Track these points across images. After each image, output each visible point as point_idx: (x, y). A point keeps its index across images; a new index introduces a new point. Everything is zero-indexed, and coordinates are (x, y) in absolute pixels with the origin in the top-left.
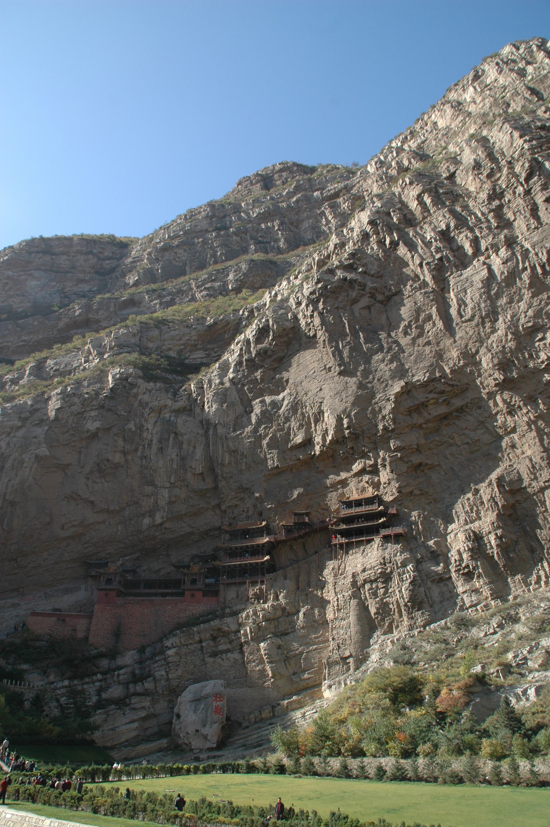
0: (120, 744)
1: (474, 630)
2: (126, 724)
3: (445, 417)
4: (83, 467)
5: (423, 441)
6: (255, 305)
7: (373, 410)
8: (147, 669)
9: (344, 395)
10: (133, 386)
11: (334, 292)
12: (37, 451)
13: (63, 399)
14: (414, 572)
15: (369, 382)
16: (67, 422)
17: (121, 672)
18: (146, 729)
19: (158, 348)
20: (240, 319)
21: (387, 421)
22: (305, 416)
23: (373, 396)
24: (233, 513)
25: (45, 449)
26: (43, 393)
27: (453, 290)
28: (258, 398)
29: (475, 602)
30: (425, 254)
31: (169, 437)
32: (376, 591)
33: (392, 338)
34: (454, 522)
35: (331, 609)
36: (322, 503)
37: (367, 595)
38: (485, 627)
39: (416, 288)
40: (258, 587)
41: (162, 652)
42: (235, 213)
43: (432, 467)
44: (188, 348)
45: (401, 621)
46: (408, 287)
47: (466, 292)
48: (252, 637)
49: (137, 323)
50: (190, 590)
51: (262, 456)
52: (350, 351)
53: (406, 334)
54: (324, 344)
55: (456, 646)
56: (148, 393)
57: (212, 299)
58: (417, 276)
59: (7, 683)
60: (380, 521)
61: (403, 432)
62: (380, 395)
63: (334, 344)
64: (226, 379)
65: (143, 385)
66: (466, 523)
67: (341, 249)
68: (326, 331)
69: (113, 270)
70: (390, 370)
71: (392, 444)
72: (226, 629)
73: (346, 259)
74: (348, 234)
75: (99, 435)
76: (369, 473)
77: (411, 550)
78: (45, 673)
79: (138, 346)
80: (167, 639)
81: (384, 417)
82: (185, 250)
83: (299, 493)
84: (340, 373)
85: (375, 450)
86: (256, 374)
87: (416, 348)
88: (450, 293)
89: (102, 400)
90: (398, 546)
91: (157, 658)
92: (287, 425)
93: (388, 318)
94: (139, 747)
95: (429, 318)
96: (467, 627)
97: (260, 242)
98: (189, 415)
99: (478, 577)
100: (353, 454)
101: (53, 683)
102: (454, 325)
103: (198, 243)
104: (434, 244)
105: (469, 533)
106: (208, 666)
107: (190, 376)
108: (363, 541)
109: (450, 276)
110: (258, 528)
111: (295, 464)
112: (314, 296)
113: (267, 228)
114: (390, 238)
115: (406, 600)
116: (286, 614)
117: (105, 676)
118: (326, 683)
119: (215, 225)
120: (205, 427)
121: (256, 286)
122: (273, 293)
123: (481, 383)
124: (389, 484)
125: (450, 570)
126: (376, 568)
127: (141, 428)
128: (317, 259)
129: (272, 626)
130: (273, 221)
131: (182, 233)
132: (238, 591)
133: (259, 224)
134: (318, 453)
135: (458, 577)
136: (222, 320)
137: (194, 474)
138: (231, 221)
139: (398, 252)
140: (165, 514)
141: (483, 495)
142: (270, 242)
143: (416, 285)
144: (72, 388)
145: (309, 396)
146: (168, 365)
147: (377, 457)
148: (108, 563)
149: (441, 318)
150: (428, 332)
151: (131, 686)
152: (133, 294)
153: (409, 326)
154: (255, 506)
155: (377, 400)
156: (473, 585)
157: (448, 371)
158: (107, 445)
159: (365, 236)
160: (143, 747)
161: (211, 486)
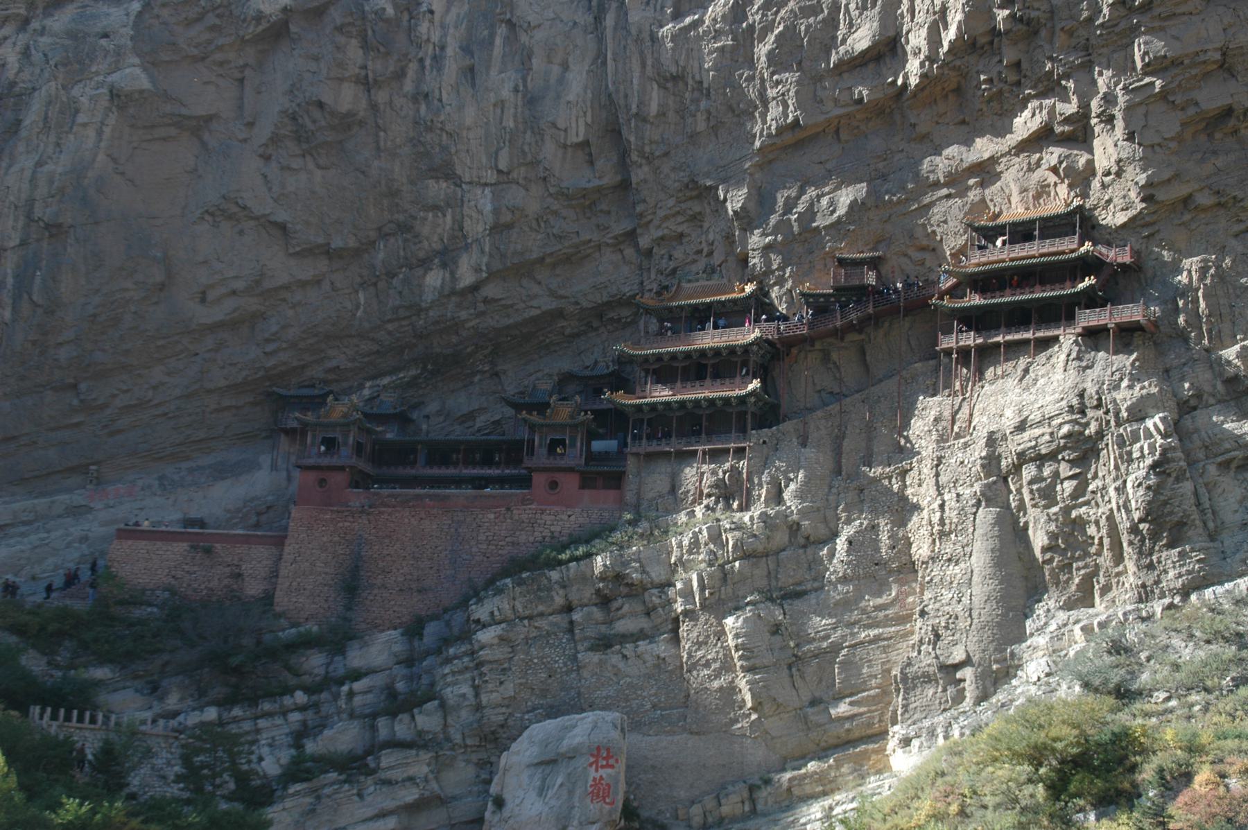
4: (251, 125)
8: (425, 680)
12: (115, 77)
14: (1164, 436)
17: (357, 686)
25: (138, 71)
31: (492, 36)
32: (1052, 487)
36: (919, 233)
37: (1027, 497)
40: (727, 466)
41: (465, 635)
45: (1118, 574)
48: (703, 599)
50: (545, 470)
51: (753, 94)
59: (41, 718)
60: (1081, 286)
75: (293, 28)
77: (1167, 371)
80: (480, 601)
83: (853, 205)
90: (1126, 361)
91: (452, 651)
100: (1018, 84)
101: (175, 714)
106: (585, 673)
108: (1026, 342)
110: (734, 301)
111: (849, 116)
115: (1136, 516)
116: (802, 541)
117: (315, 698)
118: (897, 731)
124: (1119, 174)
126: (1056, 422)
129: (760, 572)
134: (914, 81)
137: (565, 146)
140: (485, 259)
151: (382, 722)
158: (316, 59)
161: (610, 178)
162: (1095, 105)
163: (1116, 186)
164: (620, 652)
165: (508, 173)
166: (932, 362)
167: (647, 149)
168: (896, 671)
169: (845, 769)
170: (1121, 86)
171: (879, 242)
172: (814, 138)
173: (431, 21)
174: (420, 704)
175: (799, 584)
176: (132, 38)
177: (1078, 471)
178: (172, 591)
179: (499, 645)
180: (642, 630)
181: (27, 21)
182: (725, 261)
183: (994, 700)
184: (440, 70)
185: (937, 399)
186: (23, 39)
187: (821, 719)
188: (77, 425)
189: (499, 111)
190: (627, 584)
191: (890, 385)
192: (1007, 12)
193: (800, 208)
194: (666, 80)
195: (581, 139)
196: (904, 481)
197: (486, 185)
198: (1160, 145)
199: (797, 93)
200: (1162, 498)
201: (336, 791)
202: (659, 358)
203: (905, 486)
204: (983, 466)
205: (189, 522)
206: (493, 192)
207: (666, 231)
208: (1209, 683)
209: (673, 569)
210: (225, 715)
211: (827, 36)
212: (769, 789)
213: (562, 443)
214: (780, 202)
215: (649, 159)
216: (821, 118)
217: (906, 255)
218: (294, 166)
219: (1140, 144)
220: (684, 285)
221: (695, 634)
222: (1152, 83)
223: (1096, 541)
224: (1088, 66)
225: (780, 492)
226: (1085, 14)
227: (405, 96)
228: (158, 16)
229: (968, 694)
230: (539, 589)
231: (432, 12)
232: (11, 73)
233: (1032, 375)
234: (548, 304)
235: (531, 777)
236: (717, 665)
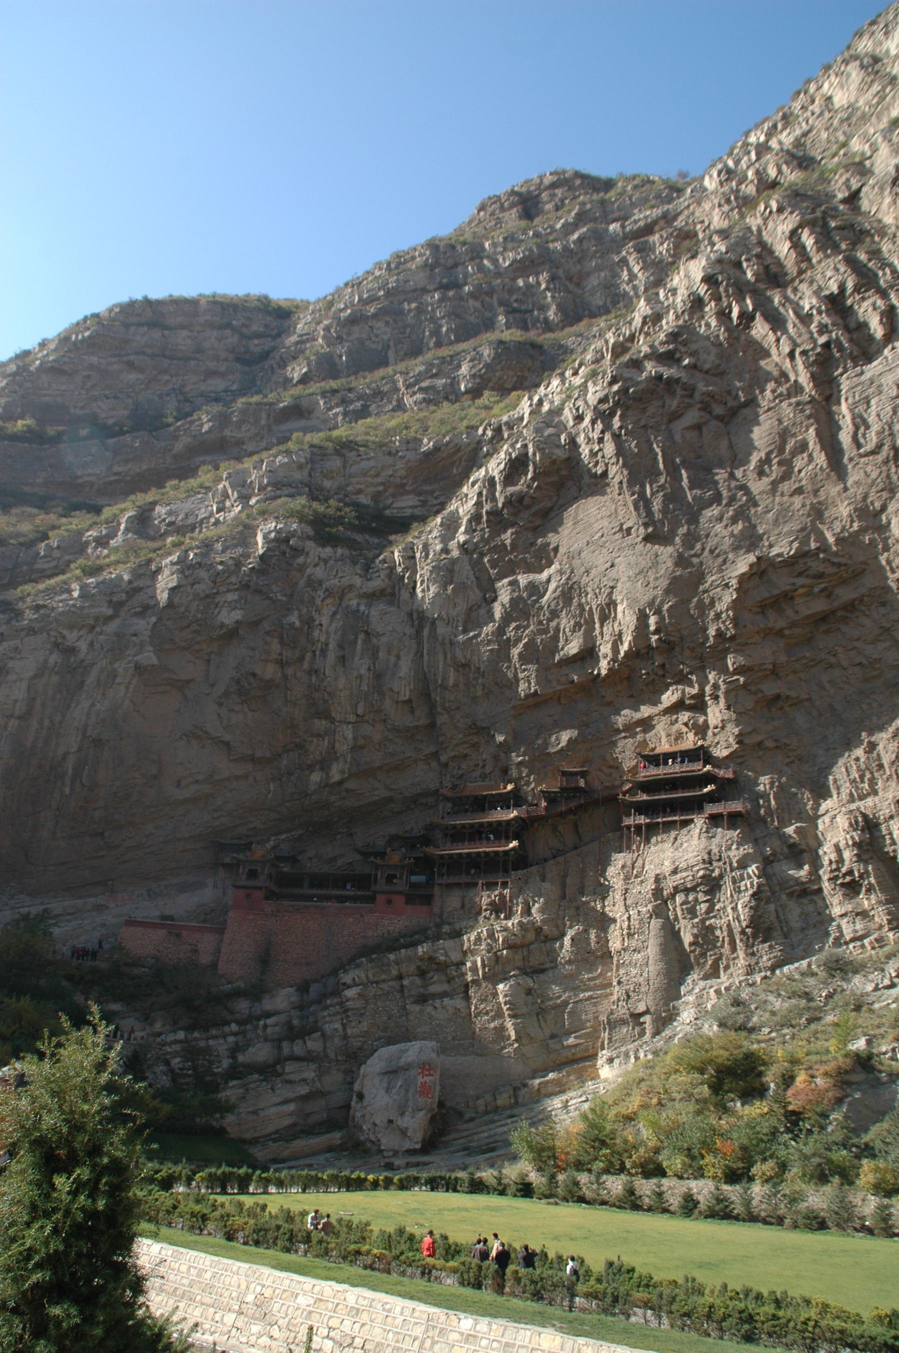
0: (266, 1136)
1: (857, 980)
3: (823, 618)
4: (212, 685)
5: (783, 658)
6: (505, 418)
8: (311, 1019)
9: (651, 575)
10: (298, 551)
11: (640, 400)
12: (139, 657)
13: (181, 572)
14: (758, 877)
15: (696, 555)
16: (187, 610)
17: (269, 1021)
18: (308, 1115)
19: (340, 488)
20: (479, 442)
21: (724, 622)
22: (584, 610)
23: (700, 577)
25: (152, 654)
26: (149, 561)
27: (847, 399)
28: (506, 577)
29: (860, 933)
30: (800, 336)
31: (356, 639)
32: (694, 907)
33: (738, 480)
34: (831, 796)
35: (617, 933)
36: (608, 757)
37: (679, 913)
38: (876, 976)
39: (781, 395)
40: (497, 892)
41: (337, 992)
42: (472, 259)
43: (797, 703)
44: (391, 490)
45: (734, 959)
46: (768, 393)
47: (868, 403)
48: (484, 973)
49: (306, 447)
51: (510, 675)
52: (663, 501)
53: (761, 473)
54: (621, 488)
55: (826, 1004)
56: (322, 564)
57: (432, 408)
58: (784, 375)
60: (705, 790)
61: (750, 641)
62: (714, 578)
63: (637, 488)
64: (453, 544)
65: (315, 551)
66: (852, 799)
67: (654, 325)
68: (624, 465)
69: (266, 355)
70: (732, 535)
72: (442, 958)
73: (662, 343)
74: (667, 299)
75: (241, 632)
76: (690, 708)
78: (147, 1017)
79: (306, 485)
80: (346, 971)
81: (718, 616)
82: (387, 323)
84: (647, 539)
85: (701, 670)
86: (503, 537)
87: (777, 499)
88: (839, 404)
89: (245, 574)
90: (735, 834)
91: (328, 1002)
92: (553, 624)
93: (731, 446)
95: (803, 447)
96: (846, 973)
97: (515, 311)
98: (391, 603)
99: (868, 891)
100: (664, 676)
101: (160, 1034)
102: (845, 460)
103: (410, 311)
104: (817, 318)
105: (856, 817)
107: (392, 538)
108: (675, 822)
109: (842, 375)
110: (500, 794)
112: (606, 406)
113: (528, 286)
114: (740, 307)
115: (744, 924)
117: (243, 1028)
118: (604, 1055)
119: (438, 280)
120: (416, 623)
121: (506, 386)
122: (536, 399)
123: (889, 562)
124: (723, 728)
125: (819, 878)
127: (309, 622)
128: (612, 341)
129: (518, 957)
130: (537, 274)
131: (382, 293)
132: (463, 898)
133: (514, 279)
134: (604, 672)
136: (448, 443)
137: (397, 702)
138: (466, 275)
139: (753, 332)
141: (882, 753)
142: (532, 311)
143: (782, 389)
144: (196, 554)
145: (592, 575)
146: (357, 518)
147: (703, 682)
148: (251, 843)
149: (823, 448)
150: (800, 471)
151: (285, 1045)
152: (299, 397)
153: (767, 460)
154: (496, 758)
155: (707, 585)
156: (858, 904)
157: (831, 540)
158: (253, 649)
159: (697, 303)
160: (301, 1144)
161: (423, 722)
162: (708, 689)
169: (571, 1078)
171: (585, 762)
174: (310, 1033)
175: (542, 964)
181: (93, 627)
183: (663, 1034)
184: (325, 657)
186: (90, 637)
187: (558, 1047)
197: (349, 723)
201: (258, 1086)
205: (164, 917)
208: (793, 1022)
209: (465, 953)
210: (189, 1036)
213: (395, 876)
215: (448, 710)
218: (236, 709)
220: (468, 784)
229: (648, 1031)
232: (82, 655)
233: (679, 841)
235: (381, 1081)
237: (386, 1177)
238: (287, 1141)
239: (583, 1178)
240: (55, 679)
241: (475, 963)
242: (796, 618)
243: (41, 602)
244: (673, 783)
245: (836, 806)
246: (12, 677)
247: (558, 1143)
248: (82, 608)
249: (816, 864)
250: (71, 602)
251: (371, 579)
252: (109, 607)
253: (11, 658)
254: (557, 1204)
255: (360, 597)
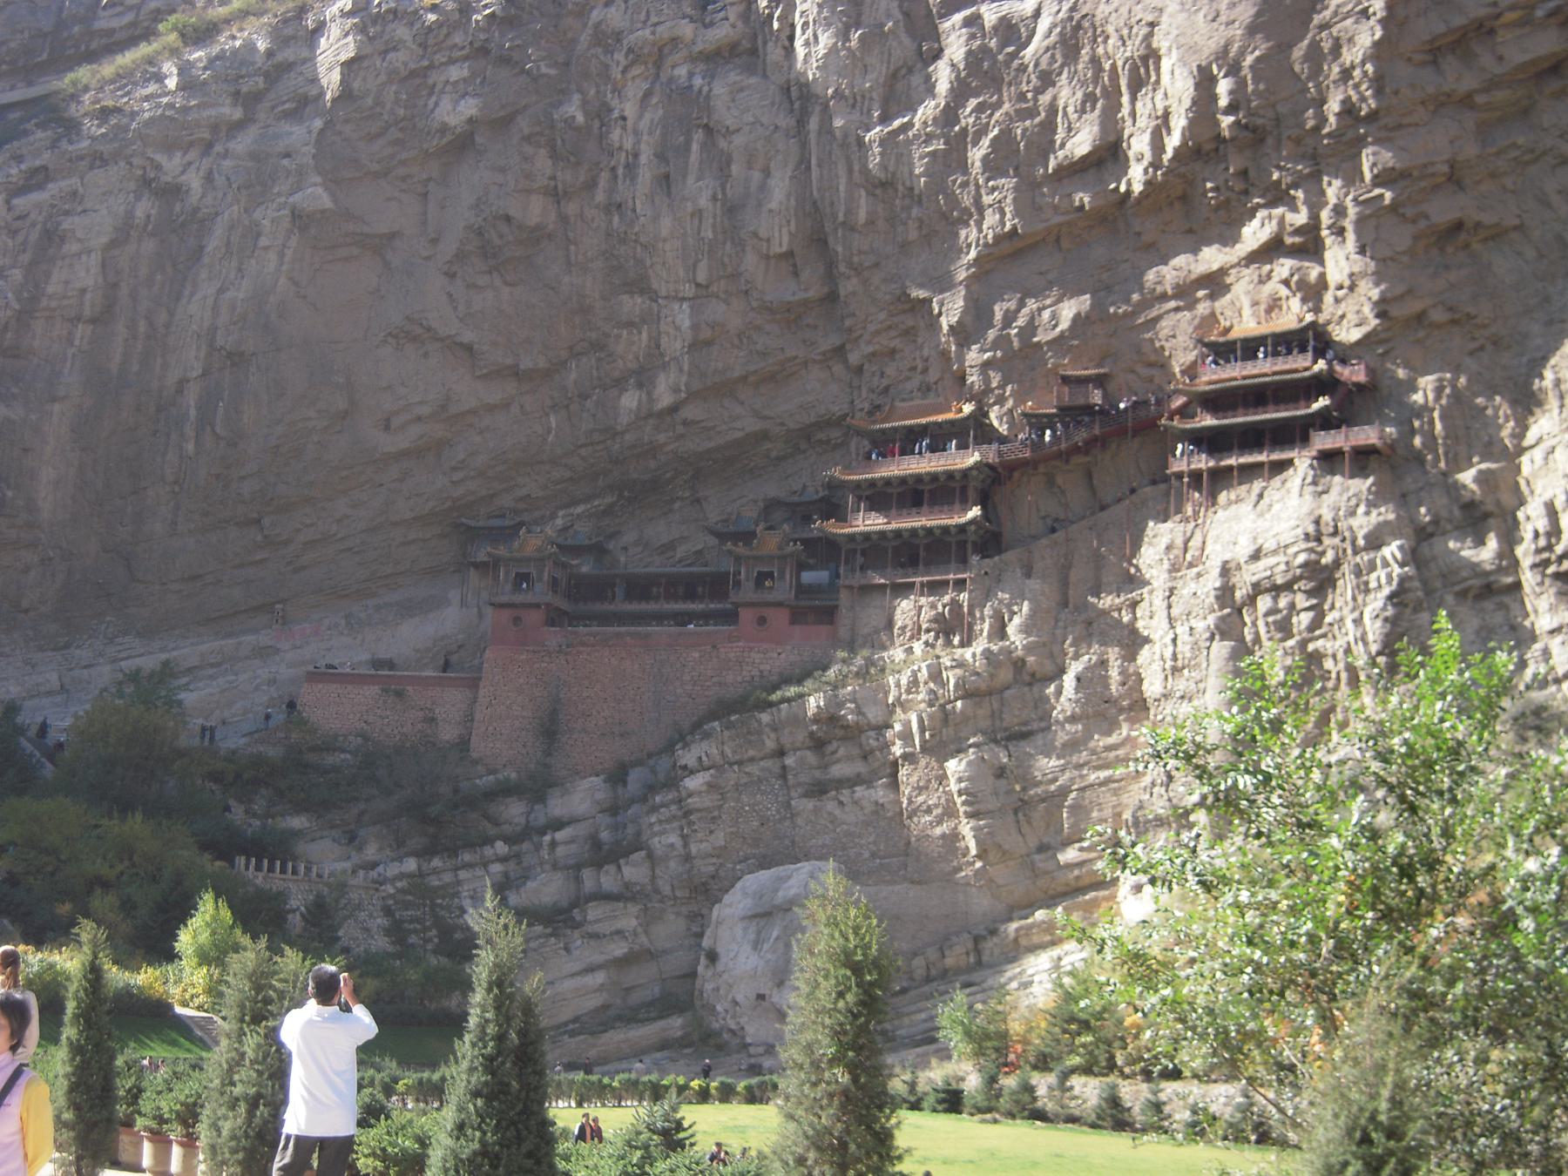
0: (558, 1027)
2: (573, 975)
4: (435, 241)
5: (1471, 150)
7: (1315, 50)
8: (630, 830)
12: (297, 197)
13: (361, 29)
14: (1402, 565)
16: (377, 104)
17: (560, 835)
18: (628, 990)
21: (1356, 86)
22: (1101, 70)
24: (882, 374)
25: (320, 190)
26: (302, 11)
28: (958, 10)
31: (688, 143)
32: (1288, 618)
35: (1157, 666)
40: (947, 599)
41: (672, 782)
43: (1497, 235)
48: (923, 742)
51: (967, 201)
59: (247, 868)
60: (1316, 406)
71: (1369, 161)
75: (479, 139)
76: (1296, 252)
77: (1404, 496)
78: (352, 838)
80: (686, 745)
81: (1346, 74)
83: (1077, 318)
89: (478, 28)
90: (1363, 485)
91: (658, 799)
92: (1045, 99)
94: (607, 1036)
96: (1548, 734)
98: (750, 70)
100: (1246, 192)
101: (374, 865)
106: (799, 821)
108: (1260, 465)
110: (952, 423)
115: (1374, 648)
116: (1027, 678)
117: (515, 848)
120: (797, 105)
124: (1352, 288)
125: (1516, 563)
126: (1292, 550)
127: (601, 114)
129: (983, 712)
134: (1137, 188)
135: (1541, 584)
137: (767, 257)
140: (684, 379)
151: (587, 874)
155: (1327, 14)
158: (503, 170)
160: (616, 1038)
162: (1325, 216)
163: (1350, 301)
164: (836, 798)
165: (707, 287)
166: (1163, 486)
167: (856, 259)
168: (1127, 815)
170: (1350, 197)
172: (1033, 247)
173: (624, 128)
174: (627, 854)
175: (1025, 723)
176: (314, 157)
177: (1314, 601)
178: (365, 737)
179: (708, 792)
180: (859, 775)
181: (209, 146)
182: (941, 379)
184: (633, 179)
185: (1169, 525)
186: (206, 163)
187: (1050, 866)
188: (261, 561)
189: (696, 222)
190: (842, 727)
191: (1118, 511)
192: (1231, 119)
193: (1021, 322)
194: (875, 187)
195: (784, 249)
196: (1134, 613)
197: (683, 299)
198: (1392, 259)
199: (1014, 199)
200: (1400, 630)
201: (543, 946)
202: (872, 483)
203: (1135, 619)
204: (1217, 598)
205: (377, 664)
206: (692, 308)
207: (877, 347)
209: (891, 710)
210: (425, 866)
211: (1045, 138)
212: (995, 939)
213: (770, 575)
214: (998, 316)
215: (857, 270)
216: (1041, 226)
217: (1133, 371)
218: (480, 282)
219: (1372, 258)
220: (898, 404)
221: (915, 778)
222: (1381, 196)
223: (1334, 675)
224: (1316, 176)
225: (1003, 626)
226: (1310, 124)
227: (597, 207)
228: (340, 133)
230: (749, 733)
231: (624, 118)
232: (194, 199)
233: (1266, 500)
234: (752, 425)
235: (745, 929)
236: (939, 811)
237: (722, 1083)
238: (592, 1034)
239: (1043, 1083)
240: (149, 246)
241: (907, 724)
242: (1498, 70)
243: (110, 103)
244: (1257, 395)
245: (1556, 430)
246: (73, 247)
247: (1015, 1027)
248: (185, 110)
249: (1510, 537)
250: (165, 100)
251: (712, 24)
252: (235, 105)
253: (67, 213)
254: (995, 1121)
255: (692, 59)
